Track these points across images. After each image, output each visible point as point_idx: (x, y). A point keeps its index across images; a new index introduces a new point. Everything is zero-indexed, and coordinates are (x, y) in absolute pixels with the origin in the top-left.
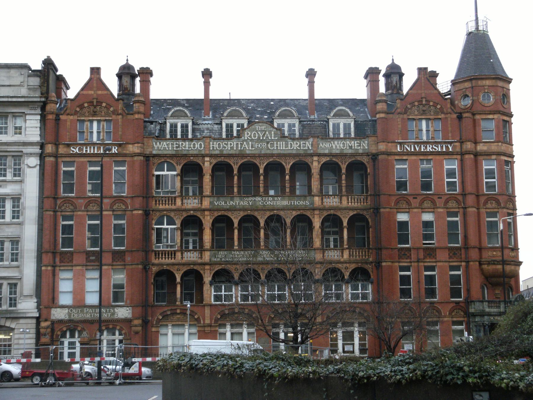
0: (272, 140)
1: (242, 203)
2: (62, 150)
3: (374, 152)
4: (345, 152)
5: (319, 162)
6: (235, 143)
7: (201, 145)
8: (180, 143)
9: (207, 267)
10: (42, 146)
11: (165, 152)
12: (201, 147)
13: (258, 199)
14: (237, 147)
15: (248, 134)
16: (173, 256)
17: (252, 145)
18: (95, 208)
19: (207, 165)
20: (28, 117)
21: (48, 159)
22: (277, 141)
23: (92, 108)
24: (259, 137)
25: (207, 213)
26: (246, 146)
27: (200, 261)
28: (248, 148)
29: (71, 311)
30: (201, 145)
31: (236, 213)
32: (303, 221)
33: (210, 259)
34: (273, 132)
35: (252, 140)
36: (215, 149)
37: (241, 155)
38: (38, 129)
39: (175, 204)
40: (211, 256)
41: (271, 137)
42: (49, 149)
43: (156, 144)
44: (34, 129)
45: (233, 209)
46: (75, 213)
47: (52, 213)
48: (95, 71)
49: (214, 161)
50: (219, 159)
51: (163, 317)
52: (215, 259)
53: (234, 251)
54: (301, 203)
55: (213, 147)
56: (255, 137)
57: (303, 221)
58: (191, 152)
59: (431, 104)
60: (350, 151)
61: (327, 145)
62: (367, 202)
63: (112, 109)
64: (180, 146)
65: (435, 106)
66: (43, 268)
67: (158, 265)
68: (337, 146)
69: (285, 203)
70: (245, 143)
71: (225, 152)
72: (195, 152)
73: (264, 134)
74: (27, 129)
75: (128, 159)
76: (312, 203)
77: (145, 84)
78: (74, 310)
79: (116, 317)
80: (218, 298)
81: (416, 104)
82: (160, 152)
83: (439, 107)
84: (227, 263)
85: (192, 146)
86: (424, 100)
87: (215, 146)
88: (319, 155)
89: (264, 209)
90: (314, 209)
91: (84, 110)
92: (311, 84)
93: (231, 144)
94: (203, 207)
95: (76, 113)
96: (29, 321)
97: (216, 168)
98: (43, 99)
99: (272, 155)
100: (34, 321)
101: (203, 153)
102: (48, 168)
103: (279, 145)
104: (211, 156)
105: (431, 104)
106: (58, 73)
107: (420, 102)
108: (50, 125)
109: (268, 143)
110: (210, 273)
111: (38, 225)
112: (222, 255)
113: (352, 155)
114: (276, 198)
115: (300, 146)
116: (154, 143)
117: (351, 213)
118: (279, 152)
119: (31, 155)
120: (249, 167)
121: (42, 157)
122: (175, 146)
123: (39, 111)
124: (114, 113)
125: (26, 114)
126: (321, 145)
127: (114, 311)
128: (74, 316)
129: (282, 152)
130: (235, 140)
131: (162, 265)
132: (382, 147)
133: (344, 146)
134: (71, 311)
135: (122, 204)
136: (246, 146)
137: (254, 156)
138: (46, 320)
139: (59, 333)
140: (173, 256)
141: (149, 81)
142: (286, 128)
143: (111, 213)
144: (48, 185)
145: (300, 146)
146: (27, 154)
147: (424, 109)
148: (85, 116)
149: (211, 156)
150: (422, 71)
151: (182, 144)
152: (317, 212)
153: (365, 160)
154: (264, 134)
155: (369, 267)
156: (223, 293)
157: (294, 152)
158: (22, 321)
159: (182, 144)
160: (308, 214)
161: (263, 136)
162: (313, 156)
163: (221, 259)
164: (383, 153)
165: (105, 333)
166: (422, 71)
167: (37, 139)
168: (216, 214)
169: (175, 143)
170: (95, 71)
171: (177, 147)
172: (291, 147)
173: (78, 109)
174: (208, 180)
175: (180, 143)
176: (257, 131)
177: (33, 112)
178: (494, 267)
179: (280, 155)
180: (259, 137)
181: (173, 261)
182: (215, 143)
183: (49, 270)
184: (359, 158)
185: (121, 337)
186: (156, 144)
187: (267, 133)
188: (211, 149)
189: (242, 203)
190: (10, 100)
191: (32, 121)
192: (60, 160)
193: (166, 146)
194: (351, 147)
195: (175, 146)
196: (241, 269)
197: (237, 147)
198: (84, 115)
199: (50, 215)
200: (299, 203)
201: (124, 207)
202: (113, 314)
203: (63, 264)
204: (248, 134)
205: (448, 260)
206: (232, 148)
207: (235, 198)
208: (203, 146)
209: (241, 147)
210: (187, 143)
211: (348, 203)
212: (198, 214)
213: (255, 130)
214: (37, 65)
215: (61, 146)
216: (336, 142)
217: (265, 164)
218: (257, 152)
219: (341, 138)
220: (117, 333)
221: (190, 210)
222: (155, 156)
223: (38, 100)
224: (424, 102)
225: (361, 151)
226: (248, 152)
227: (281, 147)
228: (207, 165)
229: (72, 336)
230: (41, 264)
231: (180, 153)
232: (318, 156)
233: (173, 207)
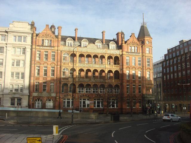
1: (87, 66)
10: (32, 46)
23: (46, 36)
40: (78, 80)
46: (40, 66)
50: (81, 53)
67: (63, 82)
80: (80, 92)
82: (65, 50)
84: (82, 82)
89: (93, 67)
96: (26, 96)
98: (32, 32)
100: (28, 96)
121: (31, 49)
123: (31, 36)
138: (31, 96)
139: (35, 100)
142: (98, 46)
153: (119, 56)
155: (119, 85)
156: (81, 90)
158: (24, 96)
160: (104, 69)
167: (30, 44)
178: (149, 85)
189: (87, 66)
196: (86, 83)
202: (51, 95)
229: (39, 101)
233: (68, 66)
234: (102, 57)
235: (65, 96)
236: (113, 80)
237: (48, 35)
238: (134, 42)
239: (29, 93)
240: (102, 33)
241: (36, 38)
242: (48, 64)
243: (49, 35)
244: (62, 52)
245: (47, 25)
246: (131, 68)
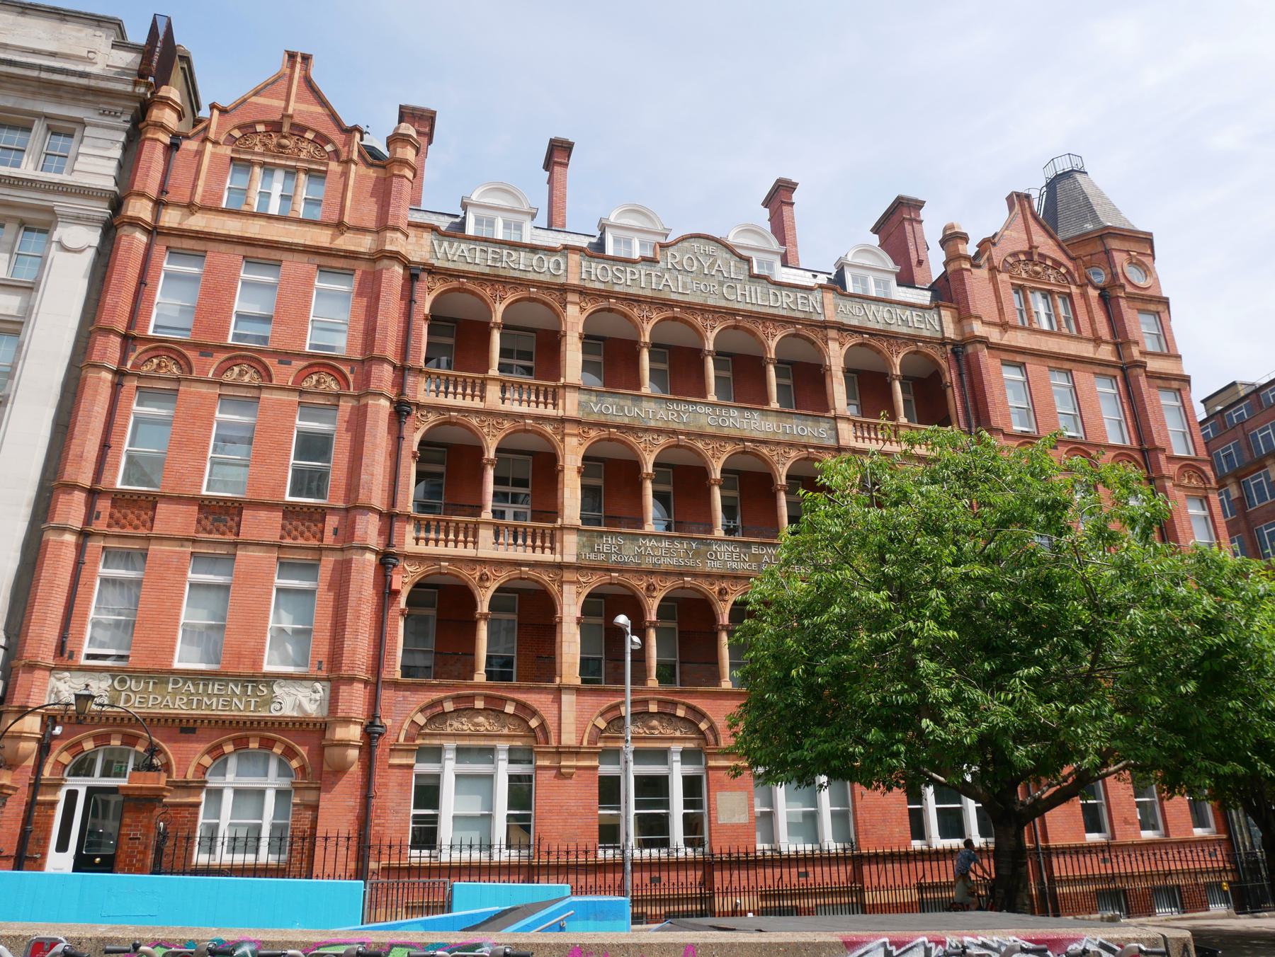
4: (894, 329)
6: (643, 272)
7: (559, 264)
8: (505, 252)
10: (117, 204)
17: (684, 283)
18: (246, 378)
20: (88, 131)
25: (569, 429)
33: (578, 555)
36: (593, 278)
38: (114, 164)
39: (482, 398)
43: (440, 246)
44: (105, 162)
51: (431, 720)
52: (592, 556)
53: (645, 536)
55: (589, 273)
60: (904, 330)
64: (504, 259)
73: (712, 264)
74: (80, 158)
79: (274, 712)
81: (1022, 257)
85: (534, 262)
87: (593, 271)
109: (721, 284)
110: (579, 593)
112: (608, 544)
119: (78, 219)
121: (110, 231)
122: (490, 256)
123: (123, 122)
128: (128, 700)
131: (437, 559)
135: (329, 379)
143: (295, 398)
146: (68, 216)
148: (254, 153)
159: (510, 255)
161: (711, 266)
162: (826, 328)
165: (232, 763)
169: (490, 250)
182: (593, 265)
185: (285, 783)
187: (719, 262)
190: (44, 75)
194: (905, 322)
195: (490, 256)
200: (803, 430)
201: (334, 386)
203: (116, 530)
208: (563, 267)
220: (273, 766)
222: (432, 271)
223: (129, 88)
231: (501, 272)
235: (437, 716)
245: (292, 56)
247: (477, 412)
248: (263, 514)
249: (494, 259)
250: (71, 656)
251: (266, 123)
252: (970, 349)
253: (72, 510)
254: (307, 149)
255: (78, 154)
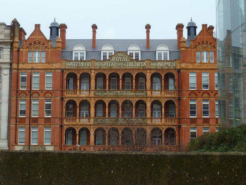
0: (126, 62)
2: (21, 66)
3: (179, 68)
4: (164, 68)
5: (150, 73)
7: (90, 64)
8: (79, 63)
9: (92, 126)
11: (72, 68)
12: (90, 65)
13: (118, 92)
14: (108, 65)
15: (114, 58)
16: (75, 121)
17: (116, 64)
19: (93, 75)
20: (4, 50)
21: (13, 71)
22: (129, 62)
24: (120, 60)
26: (113, 65)
27: (88, 124)
28: (114, 65)
29: (24, 147)
30: (90, 64)
31: (107, 99)
32: (141, 104)
34: (127, 58)
35: (116, 61)
37: (110, 69)
41: (126, 60)
42: (15, 66)
43: (67, 63)
45: (105, 97)
47: (15, 98)
48: (37, 26)
49: (96, 72)
50: (99, 71)
54: (141, 94)
55: (96, 65)
56: (117, 60)
57: (141, 104)
58: (85, 68)
59: (209, 43)
60: (166, 68)
61: (155, 64)
62: (174, 94)
63: (45, 46)
64: (79, 64)
65: (211, 44)
66: (11, 126)
67: (67, 125)
68: (160, 65)
69: (132, 94)
70: (112, 63)
71: (102, 68)
72: (87, 68)
73: (122, 58)
75: (53, 71)
76: (146, 94)
77: (63, 32)
78: (26, 147)
82: (69, 68)
83: (212, 45)
86: (205, 41)
88: (150, 69)
89: (122, 97)
90: (147, 98)
91: (32, 46)
92: (148, 32)
93: (105, 64)
94: (90, 96)
95: (28, 47)
97: (97, 76)
98: (11, 41)
99: (126, 69)
101: (91, 68)
102: (14, 76)
103: (130, 64)
104: (95, 70)
105: (209, 43)
106: (20, 27)
107: (203, 42)
108: (15, 54)
109: (124, 63)
111: (9, 104)
113: (168, 69)
114: (128, 92)
115: (140, 65)
116: (66, 63)
117: (166, 100)
118: (130, 68)
120: (114, 75)
121: (11, 69)
123: (9, 47)
124: (46, 47)
125: (3, 48)
126: (151, 64)
127: (45, 148)
129: (131, 68)
130: (107, 61)
132: (183, 65)
133: (163, 65)
134: (24, 147)
135: (49, 94)
136: (113, 65)
137: (117, 70)
140: (75, 121)
141: (65, 31)
143: (44, 98)
144: (14, 84)
145: (140, 65)
146: (4, 68)
147: (205, 46)
149: (95, 70)
150: (204, 26)
151: (80, 63)
152: (149, 99)
154: (122, 58)
155: (175, 128)
157: (138, 68)
159: (80, 63)
160: (144, 99)
163: (99, 122)
164: (184, 69)
166: (204, 26)
167: (9, 61)
168: (97, 99)
170: (37, 26)
171: (77, 65)
172: (136, 65)
173: (29, 46)
174: (93, 82)
175: (79, 63)
176: (118, 57)
177: (7, 47)
179: (130, 69)
180: (120, 60)
181: (75, 123)
182: (97, 63)
183: (14, 127)
184: (171, 71)
186: (67, 63)
187: (124, 58)
188: (95, 66)
191: (6, 52)
192: (19, 71)
193: (72, 64)
194: (167, 66)
196: (109, 127)
197: (108, 65)
198: (31, 49)
199: (15, 99)
202: (45, 149)
204: (114, 58)
205: (215, 124)
206: (106, 65)
207: (107, 91)
209: (110, 65)
210: (83, 63)
211: (165, 94)
212: (88, 99)
213: (117, 56)
214: (9, 23)
215: (20, 64)
216: (159, 63)
217: (122, 74)
218: (118, 68)
219: (162, 61)
221: (83, 97)
222: (66, 69)
224: (205, 42)
225: (172, 68)
226: (114, 68)
227: (131, 65)
228: (93, 75)
230: (10, 123)
232: (150, 70)
233: (76, 96)
234: (141, 75)
236: (163, 120)
237: (39, 43)
238: (207, 42)
239: (9, 146)
240: (146, 28)
241: (18, 51)
242: (39, 95)
243: (41, 43)
244: (64, 71)
246: (198, 93)
247: (75, 97)
248: (41, 119)
249: (77, 65)
250: (17, 144)
251: (33, 42)
252: (181, 71)
253: (13, 121)
254: (41, 46)
255: (3, 55)
